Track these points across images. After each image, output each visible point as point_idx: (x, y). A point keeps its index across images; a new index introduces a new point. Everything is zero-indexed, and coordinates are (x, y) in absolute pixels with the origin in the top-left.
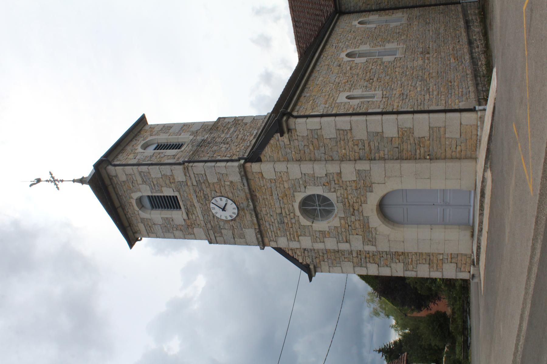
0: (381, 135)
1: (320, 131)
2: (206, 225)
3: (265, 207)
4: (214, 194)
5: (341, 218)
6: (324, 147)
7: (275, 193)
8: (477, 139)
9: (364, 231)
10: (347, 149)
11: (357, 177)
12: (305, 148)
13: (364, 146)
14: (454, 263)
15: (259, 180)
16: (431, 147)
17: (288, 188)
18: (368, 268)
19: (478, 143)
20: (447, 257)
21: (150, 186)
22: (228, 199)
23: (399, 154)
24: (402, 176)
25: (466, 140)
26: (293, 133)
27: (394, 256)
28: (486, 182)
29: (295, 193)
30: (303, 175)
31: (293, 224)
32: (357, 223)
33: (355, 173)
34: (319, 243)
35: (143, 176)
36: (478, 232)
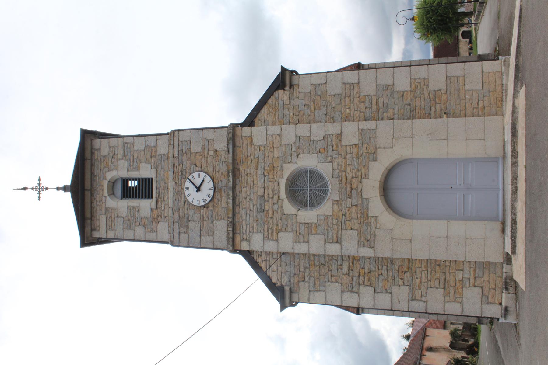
0: (391, 88)
1: (325, 85)
2: (173, 214)
3: (246, 187)
4: (193, 169)
5: (335, 202)
6: (326, 106)
7: (261, 165)
8: (503, 90)
9: (361, 222)
10: (351, 107)
11: (359, 140)
12: (305, 108)
13: (371, 104)
14: (478, 286)
15: (247, 147)
16: (448, 103)
17: (278, 157)
18: (361, 295)
19: (504, 94)
20: (469, 276)
21: (129, 162)
22: (207, 175)
23: (411, 113)
24: (413, 136)
25: (490, 92)
26: (295, 89)
27: (397, 273)
28: (518, 112)
29: (284, 164)
30: (298, 138)
31: (275, 212)
32: (354, 210)
33: (357, 133)
34: (302, 244)
35: (126, 147)
36: (512, 195)
